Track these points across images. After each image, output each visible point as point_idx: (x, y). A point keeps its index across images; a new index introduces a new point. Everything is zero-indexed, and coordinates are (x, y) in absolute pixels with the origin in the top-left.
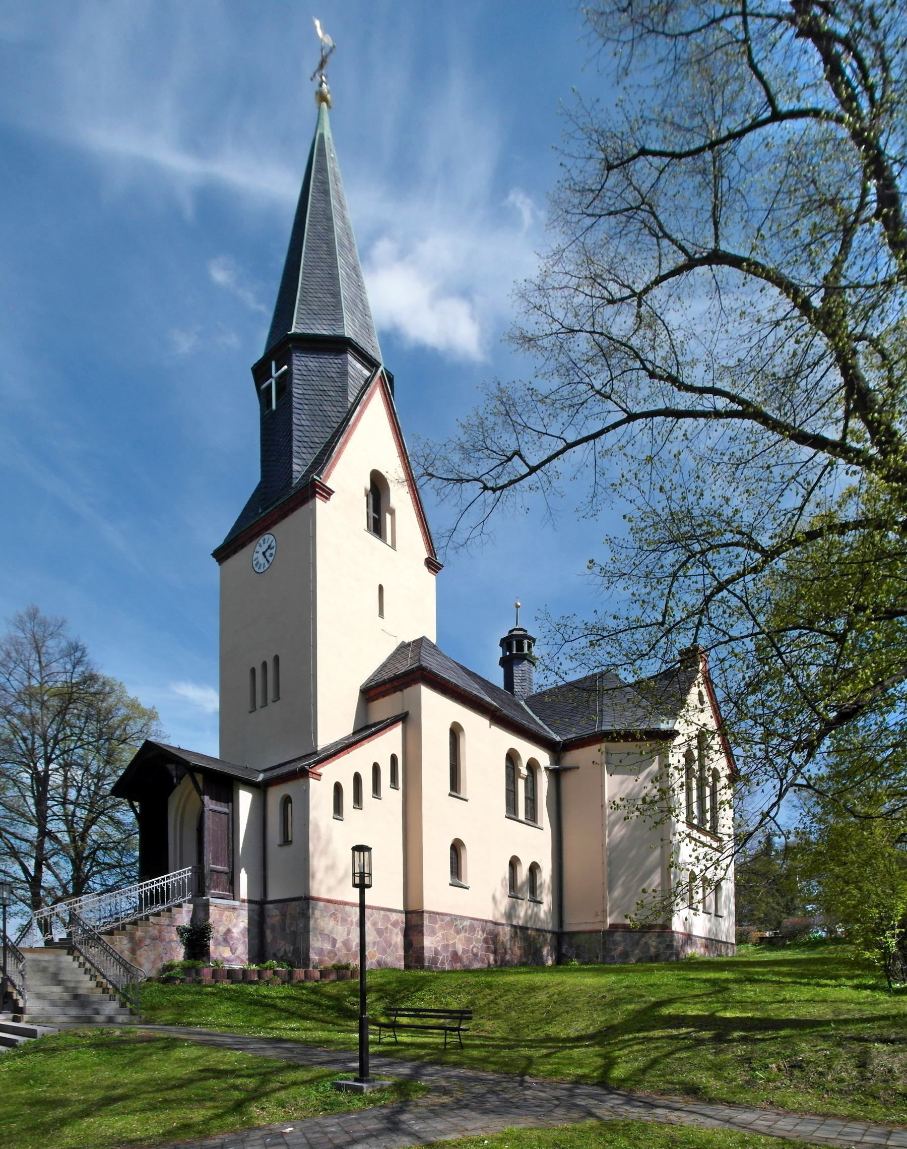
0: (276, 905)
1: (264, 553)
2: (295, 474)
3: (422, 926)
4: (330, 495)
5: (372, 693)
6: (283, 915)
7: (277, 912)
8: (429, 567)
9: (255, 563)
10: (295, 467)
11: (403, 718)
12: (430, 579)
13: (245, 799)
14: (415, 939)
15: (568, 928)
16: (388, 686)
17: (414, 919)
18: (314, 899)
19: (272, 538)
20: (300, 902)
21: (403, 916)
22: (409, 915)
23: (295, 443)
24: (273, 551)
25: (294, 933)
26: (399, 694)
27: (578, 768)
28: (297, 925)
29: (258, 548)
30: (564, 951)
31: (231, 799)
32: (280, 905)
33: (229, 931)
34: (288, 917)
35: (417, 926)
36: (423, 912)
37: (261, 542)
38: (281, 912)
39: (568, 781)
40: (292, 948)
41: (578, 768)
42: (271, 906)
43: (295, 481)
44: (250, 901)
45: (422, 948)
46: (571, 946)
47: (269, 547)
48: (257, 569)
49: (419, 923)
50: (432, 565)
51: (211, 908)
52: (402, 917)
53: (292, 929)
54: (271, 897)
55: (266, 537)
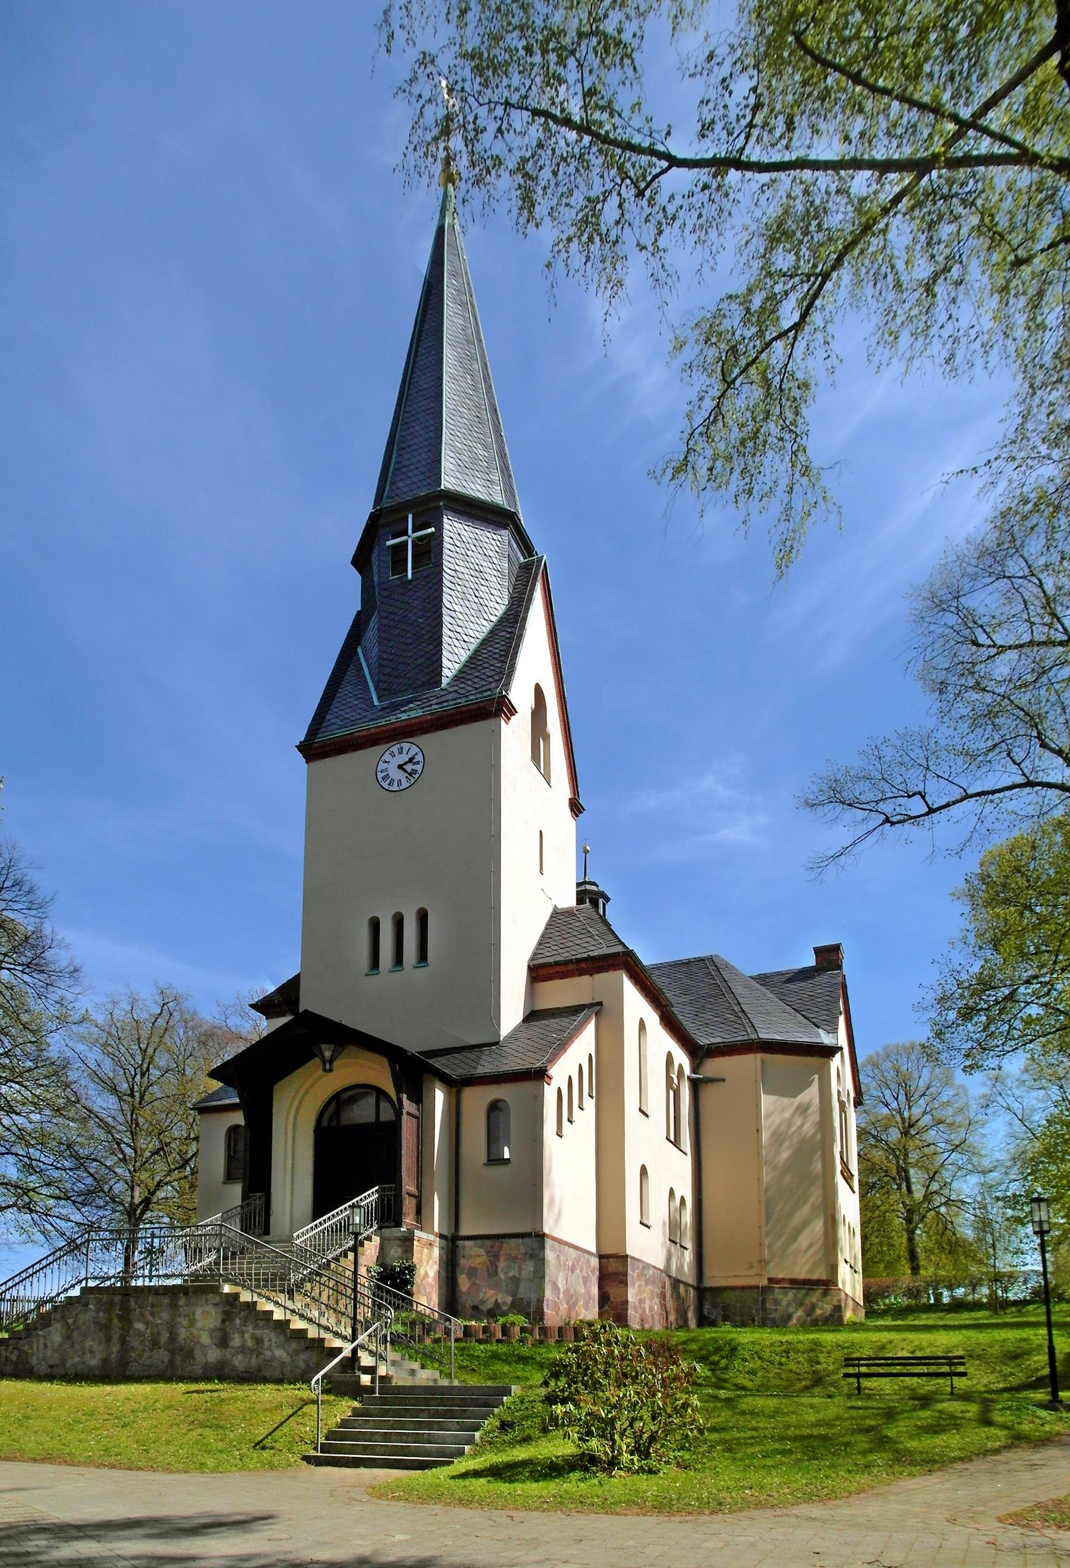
0: (479, 1242)
1: (400, 767)
2: (445, 672)
3: (626, 1274)
4: (513, 715)
5: (542, 972)
6: (494, 1257)
7: (482, 1251)
8: (572, 810)
9: (380, 776)
10: (445, 662)
11: (596, 1008)
12: (570, 823)
13: (439, 1097)
14: (613, 1292)
15: (708, 1283)
16: (571, 967)
17: (613, 1266)
18: (549, 1236)
19: (414, 750)
20: (527, 1240)
21: (597, 1260)
22: (604, 1261)
23: (445, 631)
24: (419, 768)
25: (515, 1281)
26: (587, 978)
27: (724, 1080)
28: (520, 1268)
29: (387, 757)
30: (705, 1312)
31: (419, 1097)
32: (488, 1242)
33: (426, 1273)
34: (502, 1258)
35: (617, 1274)
36: (627, 1256)
37: (395, 749)
38: (487, 1252)
39: (708, 1094)
40: (509, 1299)
41: (724, 1080)
42: (468, 1243)
43: (445, 681)
44: (441, 1236)
45: (626, 1302)
46: (715, 1305)
47: (411, 760)
48: (385, 785)
49: (621, 1269)
50: (576, 807)
51: (415, 1243)
52: (595, 1262)
53: (511, 1274)
54: (464, 1231)
55: (406, 746)
